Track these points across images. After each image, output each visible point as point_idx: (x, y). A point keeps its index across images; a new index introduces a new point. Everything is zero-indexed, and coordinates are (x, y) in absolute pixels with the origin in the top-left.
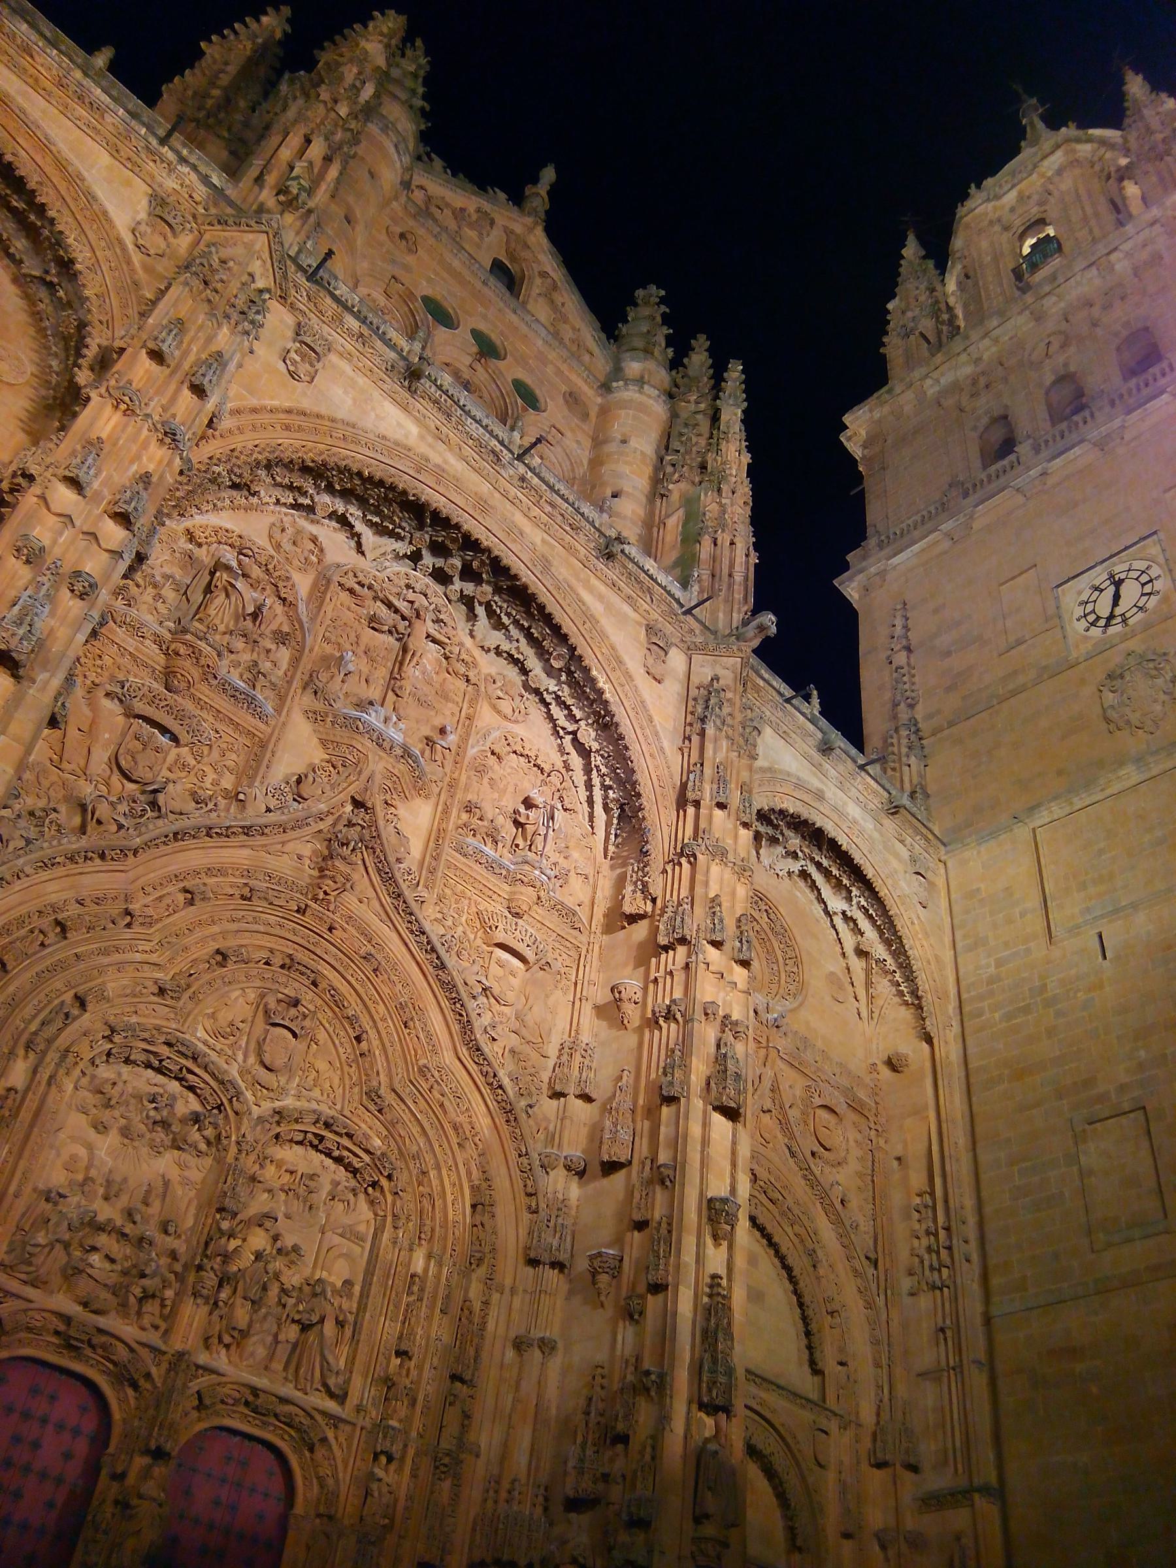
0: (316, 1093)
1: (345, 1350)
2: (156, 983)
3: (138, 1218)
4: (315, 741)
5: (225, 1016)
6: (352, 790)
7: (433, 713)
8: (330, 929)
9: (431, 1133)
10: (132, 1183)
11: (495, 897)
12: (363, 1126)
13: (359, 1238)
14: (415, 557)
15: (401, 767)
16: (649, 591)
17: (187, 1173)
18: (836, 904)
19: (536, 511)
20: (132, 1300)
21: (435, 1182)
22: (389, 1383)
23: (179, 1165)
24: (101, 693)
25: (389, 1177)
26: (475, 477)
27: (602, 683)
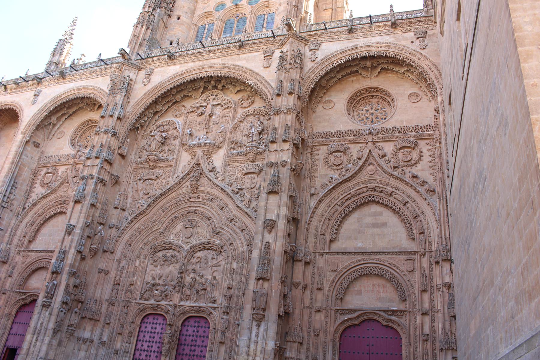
0: (201, 238)
5: (175, 232)
6: (193, 163)
8: (199, 198)
9: (232, 233)
10: (164, 275)
12: (214, 239)
14: (206, 89)
15: (207, 147)
16: (260, 43)
17: (176, 267)
18: (402, 70)
22: (225, 296)
24: (138, 181)
25: (222, 248)
26: (197, 63)
27: (250, 83)
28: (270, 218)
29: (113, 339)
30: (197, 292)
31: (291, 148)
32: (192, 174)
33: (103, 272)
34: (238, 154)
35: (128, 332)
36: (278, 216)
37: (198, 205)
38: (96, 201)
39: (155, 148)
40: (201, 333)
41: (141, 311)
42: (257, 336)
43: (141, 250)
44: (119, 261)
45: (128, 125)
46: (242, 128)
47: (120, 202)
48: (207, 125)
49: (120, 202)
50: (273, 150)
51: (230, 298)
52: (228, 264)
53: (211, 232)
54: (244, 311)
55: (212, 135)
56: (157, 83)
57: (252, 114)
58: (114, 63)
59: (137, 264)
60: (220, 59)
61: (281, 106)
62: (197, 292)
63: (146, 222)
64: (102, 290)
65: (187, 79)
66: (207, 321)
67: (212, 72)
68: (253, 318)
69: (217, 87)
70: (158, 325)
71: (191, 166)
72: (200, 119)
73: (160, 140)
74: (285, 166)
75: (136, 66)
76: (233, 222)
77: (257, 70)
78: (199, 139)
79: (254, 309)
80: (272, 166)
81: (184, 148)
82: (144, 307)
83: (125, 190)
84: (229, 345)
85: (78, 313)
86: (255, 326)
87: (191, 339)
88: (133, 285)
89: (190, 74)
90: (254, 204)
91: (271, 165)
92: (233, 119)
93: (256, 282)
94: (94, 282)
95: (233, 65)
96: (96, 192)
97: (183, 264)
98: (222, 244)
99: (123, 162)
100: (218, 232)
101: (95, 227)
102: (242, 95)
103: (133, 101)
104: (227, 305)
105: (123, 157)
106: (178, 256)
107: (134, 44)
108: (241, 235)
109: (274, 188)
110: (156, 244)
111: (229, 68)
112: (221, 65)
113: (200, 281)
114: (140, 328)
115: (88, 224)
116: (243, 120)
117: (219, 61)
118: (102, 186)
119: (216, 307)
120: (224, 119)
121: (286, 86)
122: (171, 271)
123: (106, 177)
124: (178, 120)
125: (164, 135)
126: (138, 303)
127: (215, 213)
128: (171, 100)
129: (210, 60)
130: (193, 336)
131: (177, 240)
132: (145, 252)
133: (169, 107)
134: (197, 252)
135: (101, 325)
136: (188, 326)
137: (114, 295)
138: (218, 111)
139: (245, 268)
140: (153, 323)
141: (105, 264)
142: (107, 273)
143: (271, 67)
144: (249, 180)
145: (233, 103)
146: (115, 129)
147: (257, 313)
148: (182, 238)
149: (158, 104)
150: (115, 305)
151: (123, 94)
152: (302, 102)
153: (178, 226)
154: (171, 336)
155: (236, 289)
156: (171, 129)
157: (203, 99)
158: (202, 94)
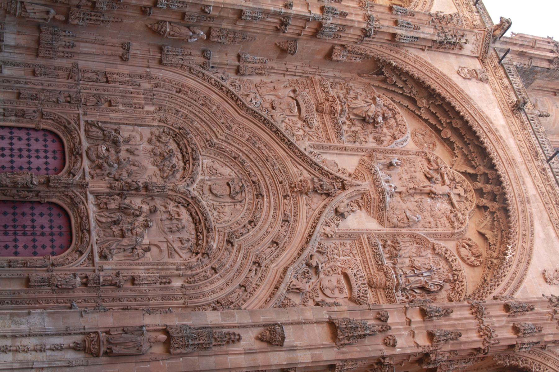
0: (216, 213)
1: (123, 258)
3: (127, 160)
4: (354, 168)
5: (217, 165)
6: (344, 178)
7: (419, 211)
8: (285, 197)
10: (137, 158)
11: (368, 270)
12: (217, 237)
13: (171, 255)
14: (472, 177)
15: (376, 197)
17: (153, 177)
19: (541, 185)
20: (97, 162)
22: (118, 275)
24: (292, 88)
25: (203, 254)
27: (509, 252)
28: (286, 336)
29: (8, 84)
30: (116, 223)
31: (420, 350)
32: (325, 180)
33: (125, 51)
34: (377, 255)
35: (25, 108)
36: (293, 349)
37: (272, 198)
38: (249, 18)
39: (354, 108)
40: (41, 240)
41: (65, 127)
42: (55, 349)
43: (174, 112)
44: (148, 77)
45: (385, 55)
46: (424, 253)
47: (249, 62)
48: (414, 191)
49: (249, 62)
50: (408, 316)
51: (115, 285)
52: (178, 269)
53: (229, 230)
54: (98, 314)
55: (399, 202)
56: (467, 92)
57: (451, 266)
58: (480, 16)
59: (147, 108)
60: (535, 192)
61: (490, 317)
62: (116, 223)
63: (223, 112)
64: (93, 54)
65: (485, 140)
66: (63, 249)
67: (509, 182)
68: (89, 334)
69: (483, 197)
70: (45, 160)
71: (338, 175)
72: (420, 176)
73: (370, 114)
74: (385, 344)
75: (486, 52)
76: (254, 267)
77: (534, 261)
78: (387, 182)
79: (108, 333)
80: (379, 319)
81: (365, 158)
82: (74, 131)
83: (273, 68)
84: (25, 296)
85: (46, 17)
86: (73, 340)
87: (26, 224)
89: (495, 144)
90: (296, 299)
91: (382, 318)
92: (434, 235)
93: (161, 328)
94: (105, 38)
95: (531, 217)
96: (263, 16)
97: (163, 188)
99: (319, 57)
100: (231, 243)
101: (202, 24)
102: (478, 244)
103: (426, 56)
104: (101, 280)
105: (329, 55)
106: (175, 177)
107: (520, 43)
108: (235, 285)
109: (342, 330)
110: (189, 136)
111: (523, 211)
112: (525, 196)
113: (136, 224)
114: (34, 129)
115: (207, 10)
116: (438, 254)
117: (532, 191)
118: (274, 25)
119: (93, 261)
120: (431, 220)
121: (527, 320)
122: (145, 169)
123: (291, 31)
124: (410, 140)
125: (380, 119)
126: (79, 120)
127: (263, 231)
128: (440, 121)
129: (528, 176)
130: (33, 227)
131: (202, 171)
132: (172, 119)
133: (426, 121)
134: (189, 210)
135: (29, 61)
136: (50, 215)
137: (87, 75)
138: (442, 206)
139: (175, 303)
140: (46, 151)
141: (138, 52)
142: (124, 59)
143: (547, 285)
144: (335, 284)
145: (462, 229)
146: (376, 33)
147: (101, 339)
148: (209, 180)
149: (428, 101)
150: (69, 81)
151: (435, 38)
152: (502, 356)
153: (228, 168)
154: (28, 187)
155: (133, 294)
156: (391, 130)
157: (456, 176)
158: (462, 173)
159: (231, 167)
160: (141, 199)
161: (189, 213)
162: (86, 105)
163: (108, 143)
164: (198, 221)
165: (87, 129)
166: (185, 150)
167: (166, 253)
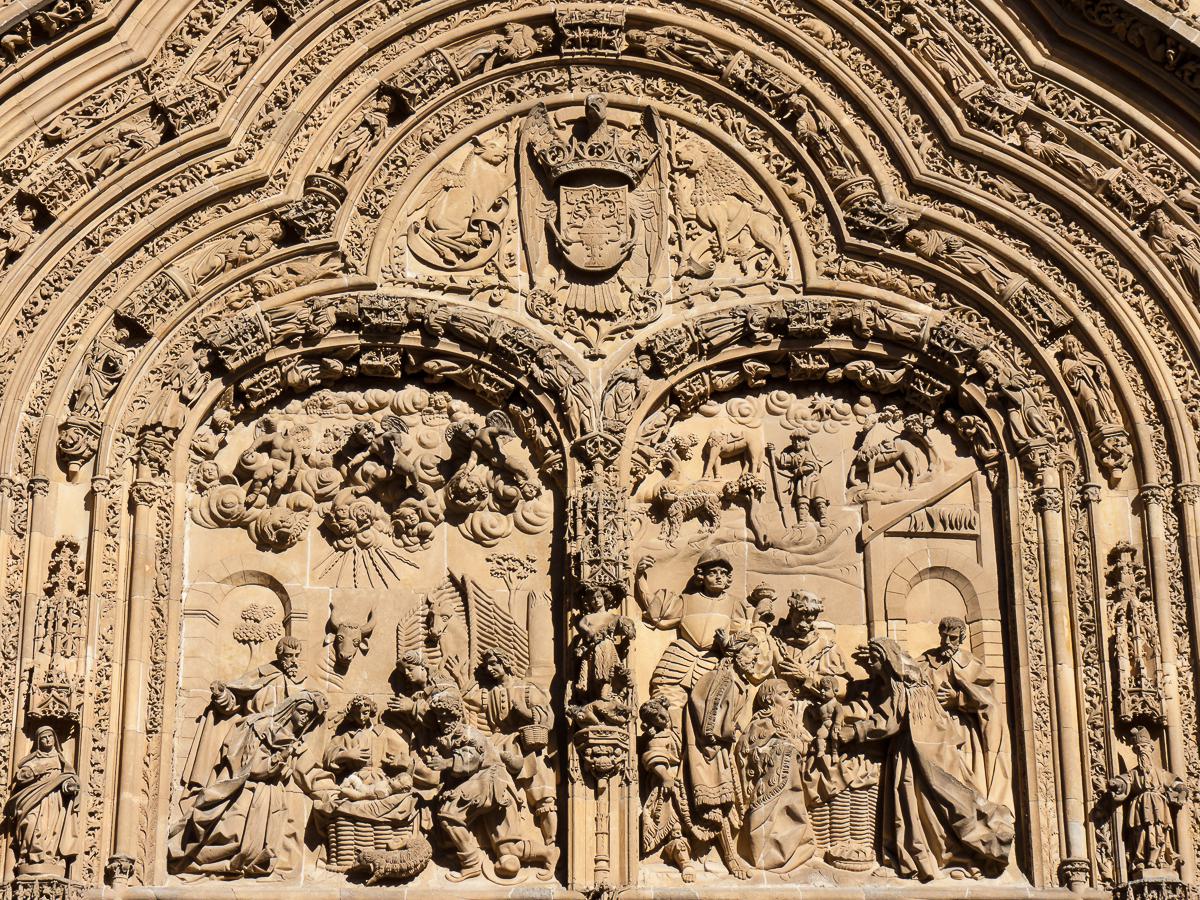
0: (725, 273)
2: (273, 218)
3: (418, 674)
5: (452, 215)
17: (502, 548)
21: (1103, 337)
23: (477, 539)
43: (99, 382)
88: (66, 727)
98: (970, 330)
100: (913, 225)
104: (1167, 874)
110: (266, 325)
153: (455, 161)
159: (451, 141)
160: (642, 629)
161: (712, 406)
162: (70, 859)
163: (304, 764)
164: (767, 369)
165: (226, 864)
166: (337, 365)
167: (958, 553)
